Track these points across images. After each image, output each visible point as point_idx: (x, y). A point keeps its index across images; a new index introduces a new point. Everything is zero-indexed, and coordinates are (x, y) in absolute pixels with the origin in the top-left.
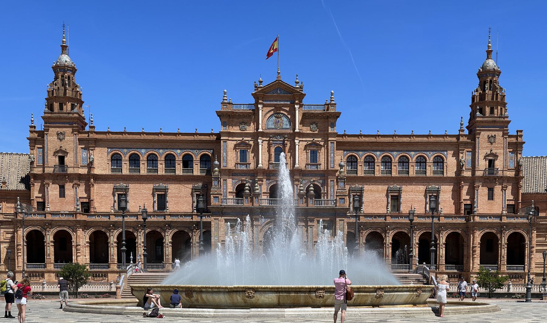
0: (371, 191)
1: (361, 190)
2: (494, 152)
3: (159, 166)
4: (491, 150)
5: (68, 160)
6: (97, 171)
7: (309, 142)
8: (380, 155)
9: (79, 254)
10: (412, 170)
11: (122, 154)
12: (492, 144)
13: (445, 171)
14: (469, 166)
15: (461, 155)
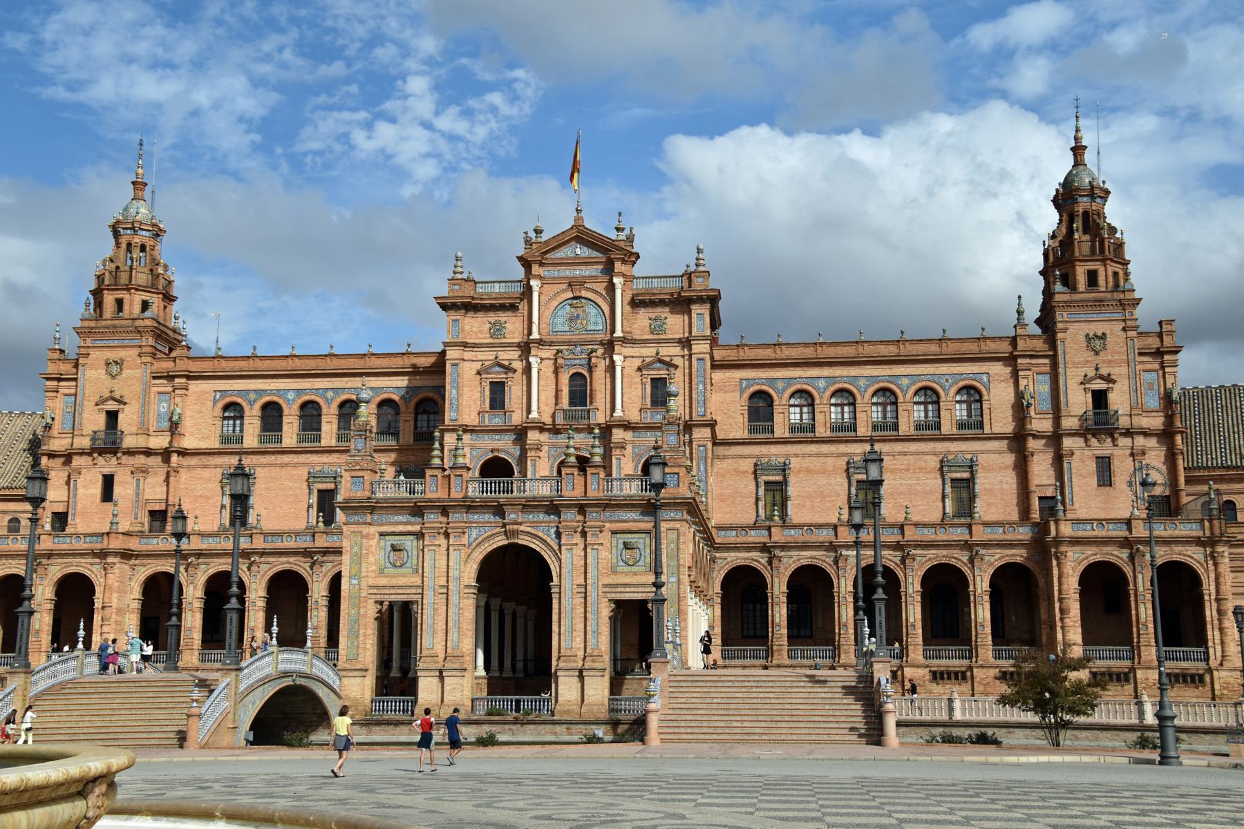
0: (808, 470)
1: (784, 470)
2: (1104, 371)
3: (325, 427)
4: (1097, 369)
5: (126, 421)
6: (188, 443)
7: (648, 360)
8: (826, 389)
9: (105, 629)
10: (905, 419)
11: (244, 404)
12: (1097, 353)
13: (986, 421)
14: (1047, 406)
15: (1023, 383)
